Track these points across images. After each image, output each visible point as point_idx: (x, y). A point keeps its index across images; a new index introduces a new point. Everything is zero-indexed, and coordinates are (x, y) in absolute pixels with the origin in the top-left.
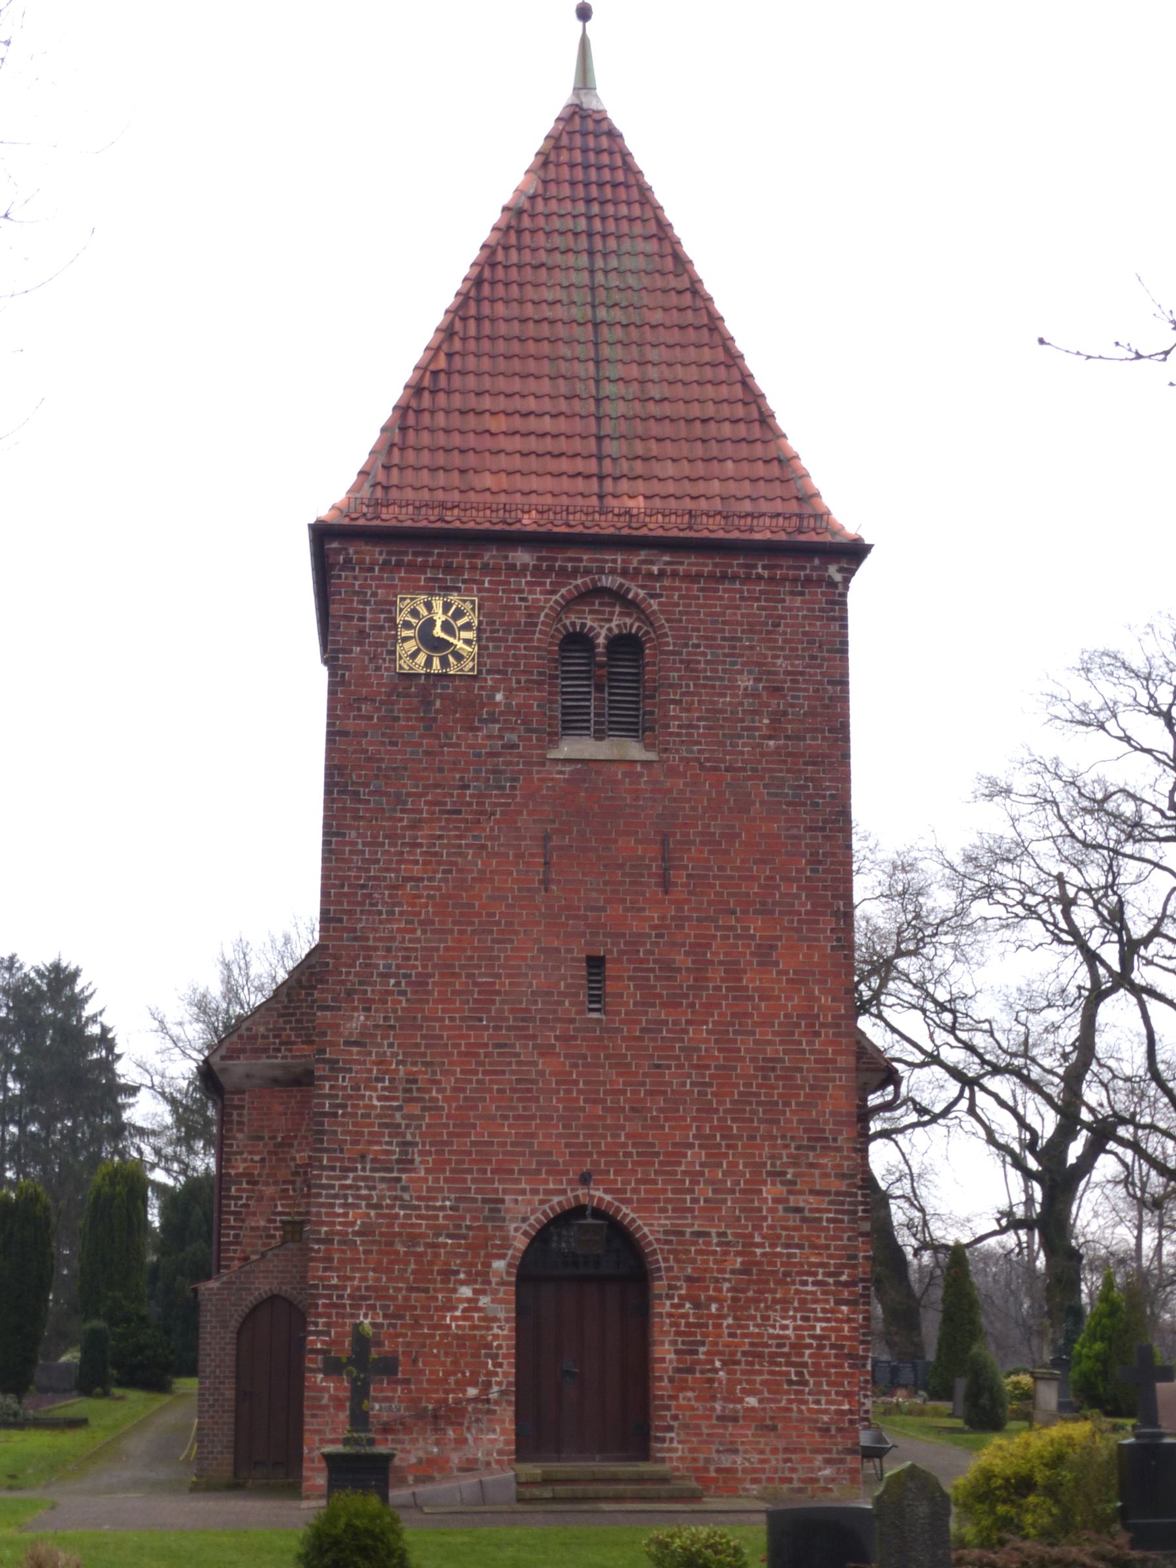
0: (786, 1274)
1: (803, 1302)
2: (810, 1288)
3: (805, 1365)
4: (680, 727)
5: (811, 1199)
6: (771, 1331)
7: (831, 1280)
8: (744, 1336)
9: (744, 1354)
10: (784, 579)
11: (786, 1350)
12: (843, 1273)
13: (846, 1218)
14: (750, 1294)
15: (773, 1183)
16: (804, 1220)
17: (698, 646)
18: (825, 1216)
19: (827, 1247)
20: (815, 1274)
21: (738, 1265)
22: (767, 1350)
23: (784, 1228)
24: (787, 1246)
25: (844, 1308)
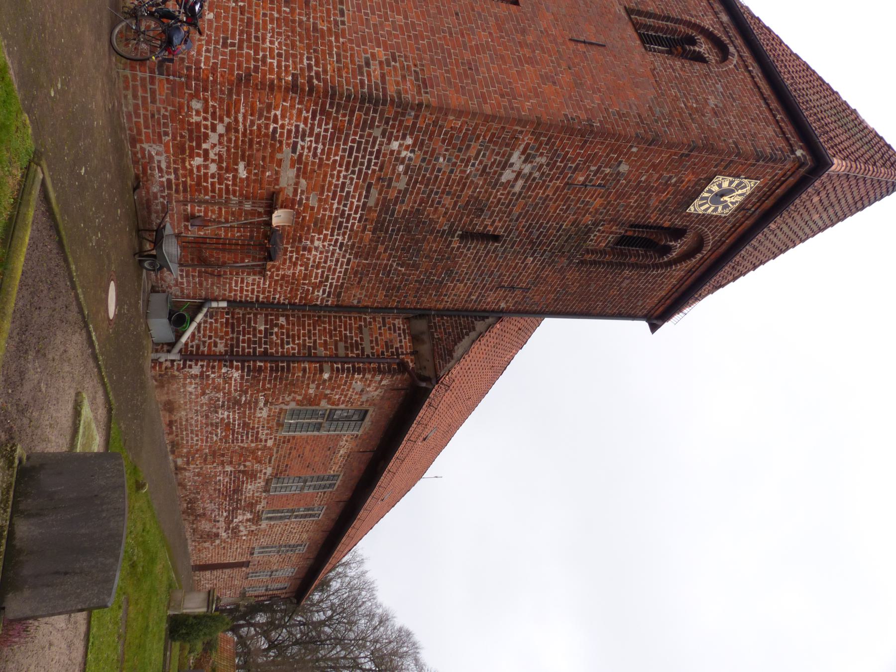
0: (316, 51)
1: (294, 56)
2: (305, 62)
3: (241, 48)
4: (670, 65)
5: (378, 72)
6: (269, 35)
7: (313, 74)
8: (265, 22)
9: (250, 19)
10: (781, 128)
11: (253, 40)
12: (319, 81)
13: (366, 90)
14: (298, 29)
15: (385, 55)
16: (360, 67)
17: (720, 81)
18: (366, 79)
19: (340, 76)
20: (317, 65)
21: (320, 27)
22: (253, 30)
23: (351, 55)
24: (338, 55)
25: (290, 78)
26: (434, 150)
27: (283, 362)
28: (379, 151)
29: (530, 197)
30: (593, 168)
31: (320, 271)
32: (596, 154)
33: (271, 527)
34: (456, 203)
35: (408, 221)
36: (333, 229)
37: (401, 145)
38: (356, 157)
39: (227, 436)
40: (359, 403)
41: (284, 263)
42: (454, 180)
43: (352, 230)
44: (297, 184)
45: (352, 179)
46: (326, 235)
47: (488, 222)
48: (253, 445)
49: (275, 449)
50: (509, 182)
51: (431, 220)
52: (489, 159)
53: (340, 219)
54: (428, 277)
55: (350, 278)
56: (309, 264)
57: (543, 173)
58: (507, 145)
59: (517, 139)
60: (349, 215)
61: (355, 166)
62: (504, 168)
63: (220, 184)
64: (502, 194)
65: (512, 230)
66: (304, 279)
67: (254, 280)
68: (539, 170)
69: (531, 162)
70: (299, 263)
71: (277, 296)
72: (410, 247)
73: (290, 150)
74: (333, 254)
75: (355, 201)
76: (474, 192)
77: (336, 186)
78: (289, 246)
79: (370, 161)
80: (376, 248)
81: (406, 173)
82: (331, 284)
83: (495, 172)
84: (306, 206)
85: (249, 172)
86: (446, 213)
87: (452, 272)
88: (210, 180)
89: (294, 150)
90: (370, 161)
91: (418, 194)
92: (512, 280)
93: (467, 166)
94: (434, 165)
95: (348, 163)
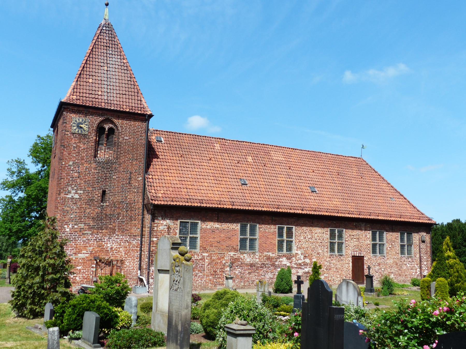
26: (68, 219)
27: (150, 253)
28: (70, 234)
29: (85, 187)
30: (72, 172)
31: (122, 243)
32: (66, 174)
33: (299, 248)
34: (88, 208)
35: (98, 220)
36: (102, 242)
37: (67, 228)
38: (72, 239)
39: (199, 270)
40: (176, 225)
41: (119, 254)
42: (79, 211)
43: (102, 236)
44: (84, 253)
45: (81, 239)
46: (105, 243)
47: (96, 196)
48: (206, 261)
49: (211, 252)
50: (79, 195)
51: (96, 214)
52: (70, 203)
53: (98, 240)
54: (125, 208)
55: (125, 234)
56: (119, 247)
57: (75, 186)
58: (65, 200)
59: (62, 198)
60: (95, 238)
61: (76, 239)
62: (74, 198)
63: (85, 273)
64: (84, 196)
65: (99, 188)
66: (127, 248)
67: (127, 263)
68: (74, 188)
69: (71, 191)
70: (118, 250)
71: (136, 255)
72: (109, 218)
73: (71, 256)
74: (113, 240)
75: (89, 237)
76: (84, 204)
77: (83, 243)
78: (110, 253)
79: (73, 235)
80: (110, 228)
81: (78, 225)
82: (128, 239)
83: (75, 200)
84: (92, 250)
85: (81, 266)
86: (93, 210)
87: (122, 201)
88: (84, 275)
89: (72, 255)
90: (73, 235)
91: (85, 220)
92: (125, 180)
93: (73, 209)
94: (74, 218)
95: (75, 241)
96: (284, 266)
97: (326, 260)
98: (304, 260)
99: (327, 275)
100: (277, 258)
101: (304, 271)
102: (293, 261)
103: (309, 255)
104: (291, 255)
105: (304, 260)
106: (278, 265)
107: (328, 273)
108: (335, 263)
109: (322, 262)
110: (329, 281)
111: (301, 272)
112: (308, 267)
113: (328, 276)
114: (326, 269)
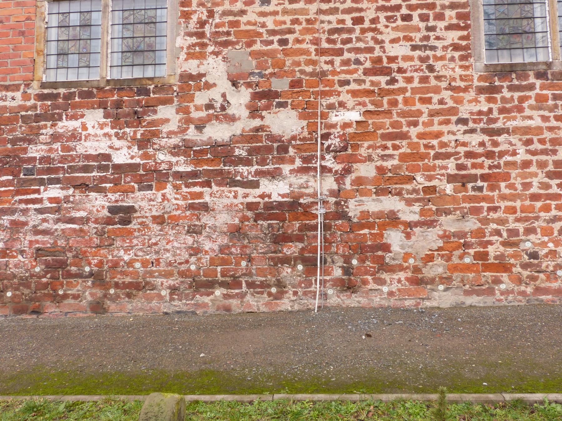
96: (86, 169)
97: (453, 111)
98: (257, 122)
99: (472, 224)
100: (38, 118)
101: (253, 196)
102: (165, 129)
103: (296, 84)
104: (146, 92)
105: (257, 122)
106: (43, 160)
107: (476, 211)
108: (539, 130)
109: (413, 132)
110: (488, 267)
111: (229, 208)
112: (286, 168)
113: (479, 233)
114: (451, 179)
